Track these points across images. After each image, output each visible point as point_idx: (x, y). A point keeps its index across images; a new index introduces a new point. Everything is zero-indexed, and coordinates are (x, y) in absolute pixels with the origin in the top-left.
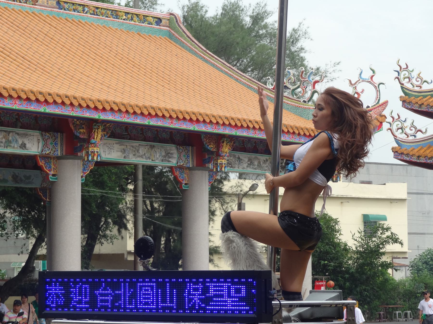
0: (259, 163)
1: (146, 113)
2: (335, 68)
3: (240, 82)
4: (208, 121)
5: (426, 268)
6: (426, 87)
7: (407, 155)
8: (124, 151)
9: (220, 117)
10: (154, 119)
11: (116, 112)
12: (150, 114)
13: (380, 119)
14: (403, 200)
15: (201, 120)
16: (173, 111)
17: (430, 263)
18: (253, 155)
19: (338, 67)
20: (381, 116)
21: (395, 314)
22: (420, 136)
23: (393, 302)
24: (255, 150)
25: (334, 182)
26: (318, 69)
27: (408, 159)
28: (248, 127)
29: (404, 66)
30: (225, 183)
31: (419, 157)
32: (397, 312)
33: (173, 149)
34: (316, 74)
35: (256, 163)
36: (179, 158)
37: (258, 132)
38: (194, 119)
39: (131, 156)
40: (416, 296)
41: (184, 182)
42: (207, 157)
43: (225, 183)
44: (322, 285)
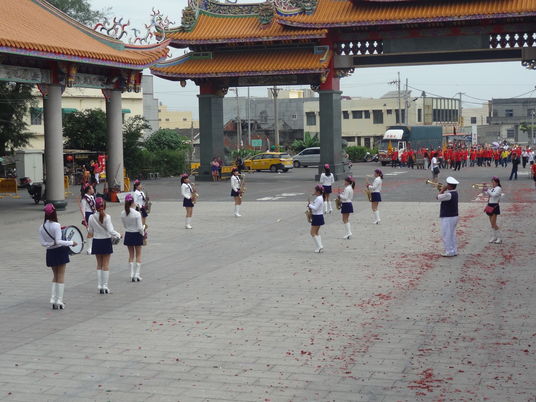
0: (91, 80)
1: (28, 48)
2: (109, 12)
3: (71, 24)
4: (65, 53)
6: (171, 26)
7: (160, 71)
8: (8, 73)
9: (72, 50)
10: (33, 52)
11: (9, 47)
12: (30, 48)
13: (166, 51)
14: (141, 99)
15: (61, 52)
16: (44, 46)
18: (87, 75)
19: (111, 11)
20: (167, 49)
22: (168, 59)
23: (145, 167)
24: (87, 72)
25: (136, 92)
26: (98, 12)
27: (160, 74)
28: (89, 57)
29: (157, 12)
30: (33, 89)
31: (167, 73)
33: (38, 71)
34: (96, 16)
35: (89, 81)
36: (43, 78)
37: (95, 60)
38: (57, 52)
39: (13, 76)
41: (46, 94)
42: (60, 77)
43: (33, 89)
44: (103, 158)
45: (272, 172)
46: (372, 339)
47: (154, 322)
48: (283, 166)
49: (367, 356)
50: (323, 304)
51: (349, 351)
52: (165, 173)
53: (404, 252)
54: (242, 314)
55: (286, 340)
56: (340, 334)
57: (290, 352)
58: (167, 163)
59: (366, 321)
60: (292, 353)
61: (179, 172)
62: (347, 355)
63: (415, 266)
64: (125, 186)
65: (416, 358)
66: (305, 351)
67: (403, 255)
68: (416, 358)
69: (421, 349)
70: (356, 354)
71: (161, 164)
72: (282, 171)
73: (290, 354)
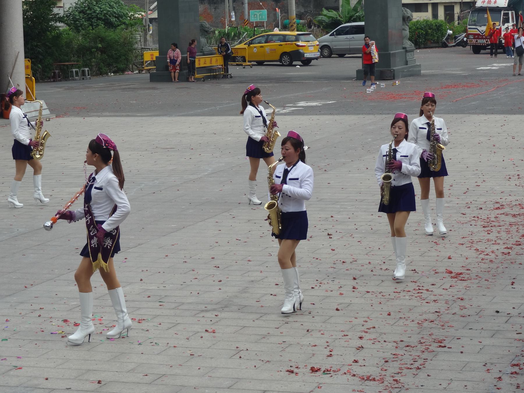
5: (83, 18)
17: (88, 12)
21: (72, 72)
32: (74, 70)
40: (91, 51)
45: (283, 65)
46: (434, 347)
47: (65, 321)
48: (303, 55)
49: (422, 374)
50: (354, 288)
51: (393, 367)
52: (100, 69)
53: (499, 200)
54: (215, 307)
55: (287, 350)
56: (379, 339)
57: (292, 369)
58: (103, 51)
59: (425, 316)
60: (296, 370)
61: (122, 66)
62: (388, 373)
63: (516, 224)
64: (27, 92)
65: (506, 379)
66: (316, 367)
67: (497, 205)
68: (506, 379)
69: (515, 362)
70: (405, 371)
71: (91, 53)
72: (300, 63)
73: (292, 372)
